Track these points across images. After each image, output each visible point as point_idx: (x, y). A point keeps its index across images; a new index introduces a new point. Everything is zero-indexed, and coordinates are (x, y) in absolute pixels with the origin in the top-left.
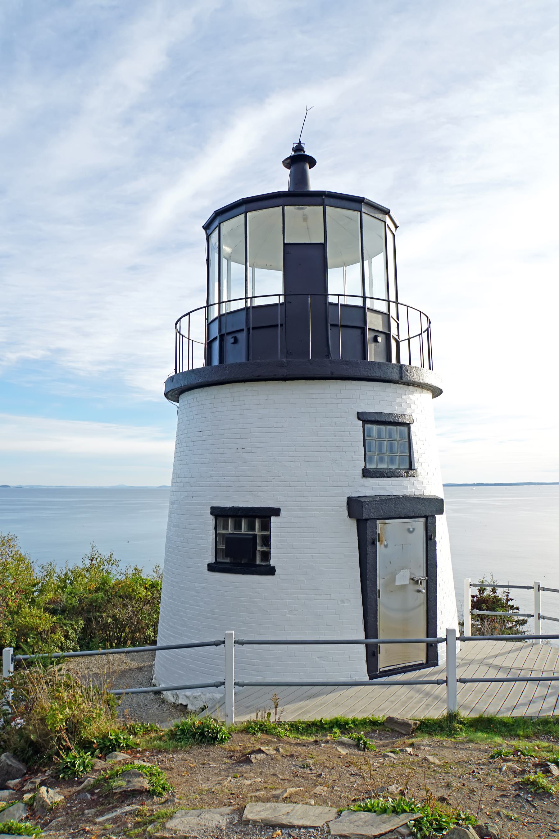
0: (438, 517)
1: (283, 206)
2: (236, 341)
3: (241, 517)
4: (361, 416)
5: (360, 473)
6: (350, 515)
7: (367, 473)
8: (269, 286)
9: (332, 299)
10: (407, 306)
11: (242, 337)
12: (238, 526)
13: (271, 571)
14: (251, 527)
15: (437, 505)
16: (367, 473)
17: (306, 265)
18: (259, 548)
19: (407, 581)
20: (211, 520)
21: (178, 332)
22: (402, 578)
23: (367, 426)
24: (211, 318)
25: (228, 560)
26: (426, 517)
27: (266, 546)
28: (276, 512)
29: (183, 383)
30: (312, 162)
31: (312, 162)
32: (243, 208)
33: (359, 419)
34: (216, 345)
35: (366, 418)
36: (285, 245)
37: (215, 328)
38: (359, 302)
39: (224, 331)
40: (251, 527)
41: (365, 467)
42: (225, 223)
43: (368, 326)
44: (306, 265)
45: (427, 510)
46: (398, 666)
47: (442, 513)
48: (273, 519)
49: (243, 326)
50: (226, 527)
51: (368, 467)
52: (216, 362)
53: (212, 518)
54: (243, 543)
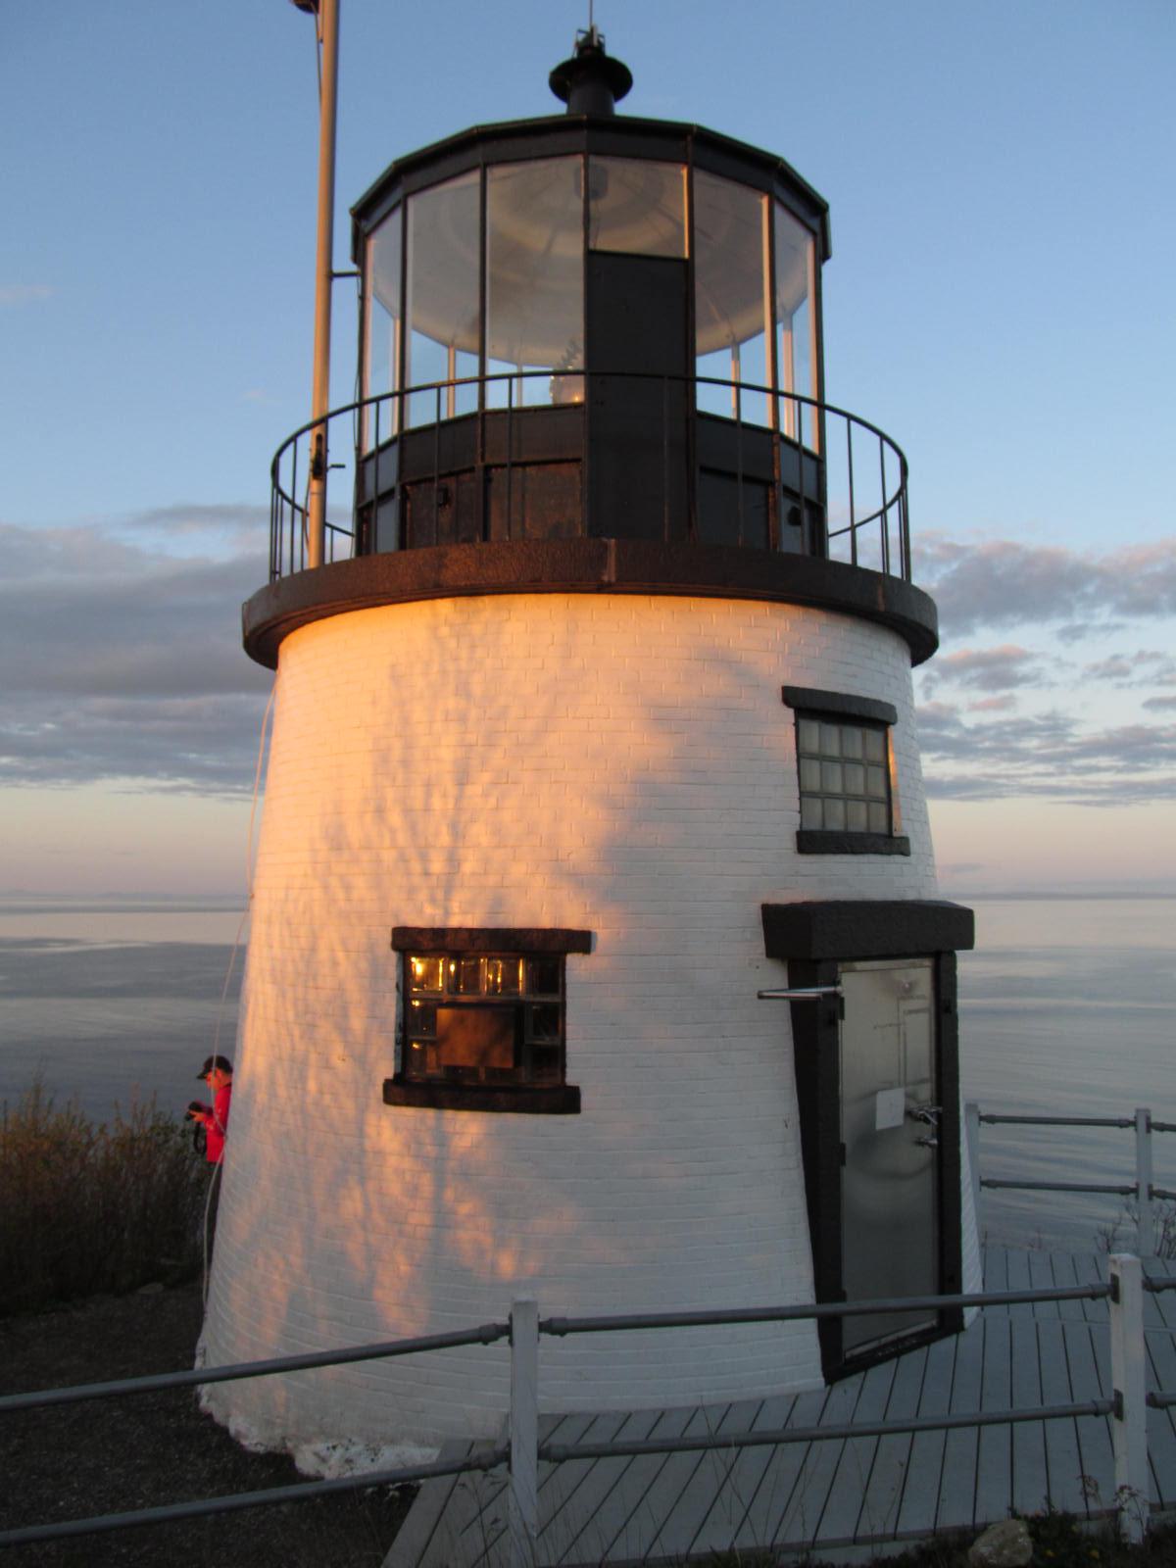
0: (959, 953)
2: (446, 499)
5: (790, 843)
6: (773, 951)
7: (809, 842)
9: (711, 401)
13: (568, 1101)
16: (809, 842)
19: (898, 1119)
22: (889, 1110)
24: (384, 438)
32: (477, 154)
36: (591, 255)
37: (390, 460)
41: (801, 825)
44: (643, 317)
46: (884, 1341)
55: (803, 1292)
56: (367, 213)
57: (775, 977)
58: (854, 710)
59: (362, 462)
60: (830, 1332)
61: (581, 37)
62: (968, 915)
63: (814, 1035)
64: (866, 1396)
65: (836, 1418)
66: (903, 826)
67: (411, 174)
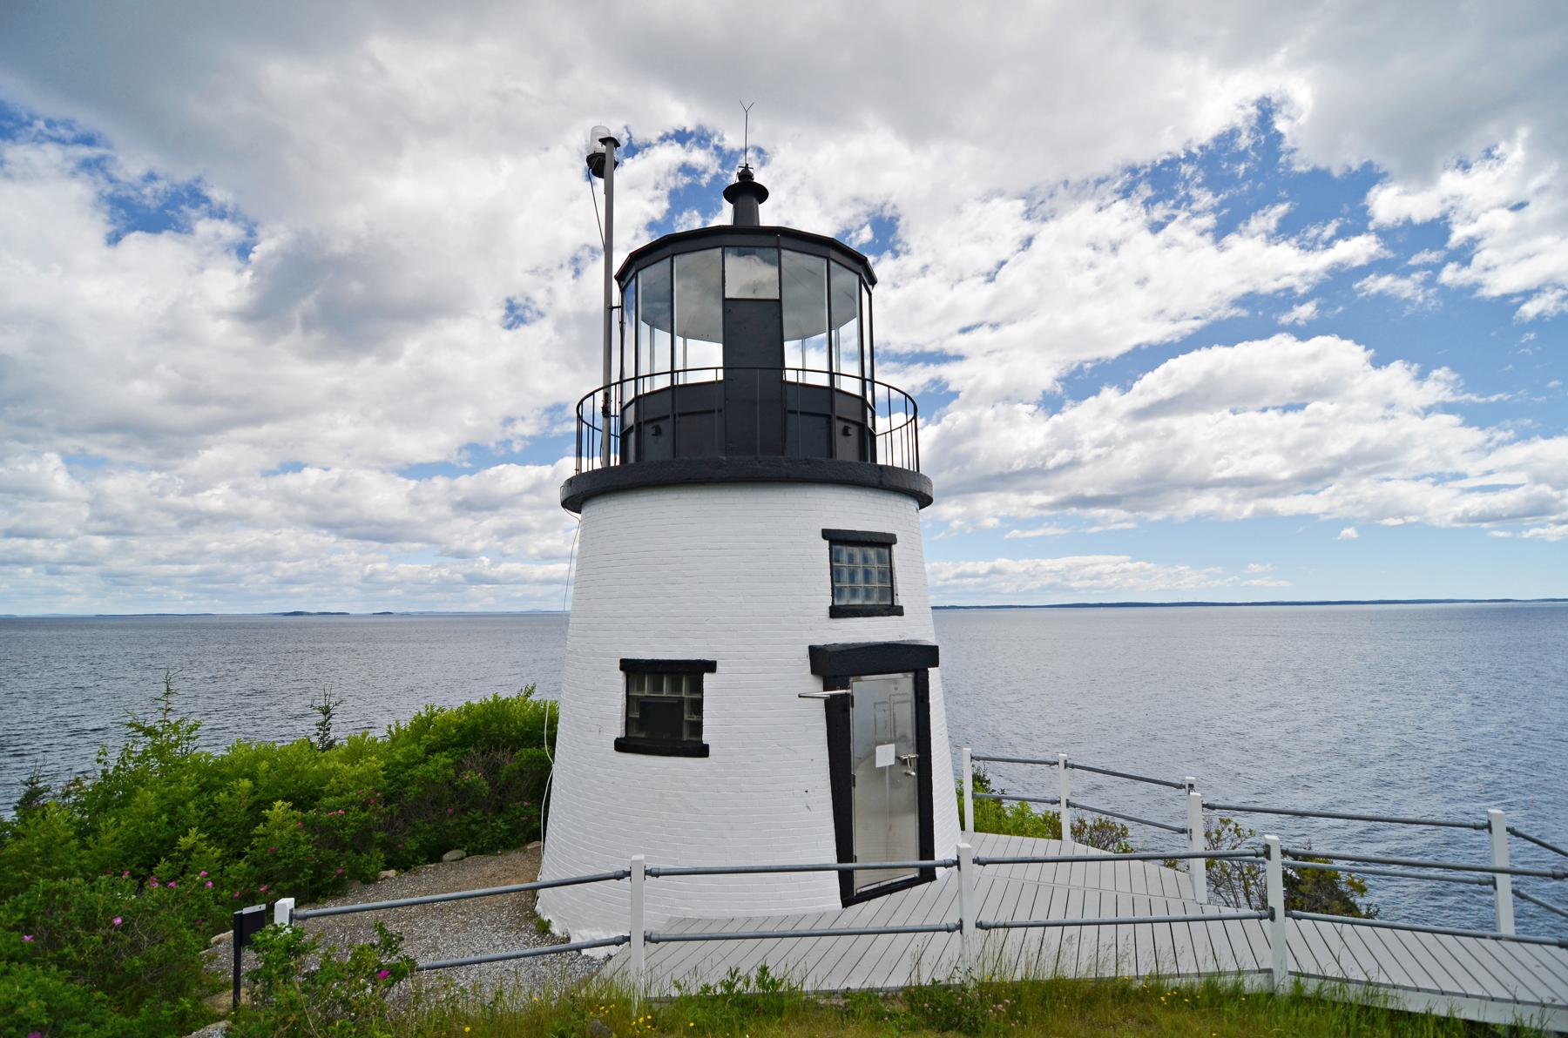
1: (724, 247)
2: (658, 432)
3: (662, 673)
4: (826, 534)
6: (813, 672)
7: (836, 612)
8: (704, 360)
9: (790, 376)
11: (666, 426)
13: (702, 751)
14: (676, 687)
15: (930, 655)
16: (836, 612)
17: (753, 331)
18: (686, 717)
20: (620, 677)
22: (885, 756)
24: (627, 400)
25: (643, 735)
28: (711, 666)
30: (761, 194)
31: (761, 194)
32: (669, 250)
34: (632, 436)
35: (835, 538)
36: (725, 300)
38: (823, 380)
40: (676, 687)
42: (645, 271)
43: (838, 412)
44: (753, 331)
45: (916, 660)
48: (706, 676)
50: (641, 688)
52: (632, 459)
53: (621, 673)
54: (664, 709)
55: (831, 857)
56: (621, 277)
57: (814, 686)
58: (862, 538)
59: (623, 410)
60: (846, 879)
62: (936, 649)
63: (838, 715)
64: (864, 913)
65: (842, 925)
67: (638, 259)
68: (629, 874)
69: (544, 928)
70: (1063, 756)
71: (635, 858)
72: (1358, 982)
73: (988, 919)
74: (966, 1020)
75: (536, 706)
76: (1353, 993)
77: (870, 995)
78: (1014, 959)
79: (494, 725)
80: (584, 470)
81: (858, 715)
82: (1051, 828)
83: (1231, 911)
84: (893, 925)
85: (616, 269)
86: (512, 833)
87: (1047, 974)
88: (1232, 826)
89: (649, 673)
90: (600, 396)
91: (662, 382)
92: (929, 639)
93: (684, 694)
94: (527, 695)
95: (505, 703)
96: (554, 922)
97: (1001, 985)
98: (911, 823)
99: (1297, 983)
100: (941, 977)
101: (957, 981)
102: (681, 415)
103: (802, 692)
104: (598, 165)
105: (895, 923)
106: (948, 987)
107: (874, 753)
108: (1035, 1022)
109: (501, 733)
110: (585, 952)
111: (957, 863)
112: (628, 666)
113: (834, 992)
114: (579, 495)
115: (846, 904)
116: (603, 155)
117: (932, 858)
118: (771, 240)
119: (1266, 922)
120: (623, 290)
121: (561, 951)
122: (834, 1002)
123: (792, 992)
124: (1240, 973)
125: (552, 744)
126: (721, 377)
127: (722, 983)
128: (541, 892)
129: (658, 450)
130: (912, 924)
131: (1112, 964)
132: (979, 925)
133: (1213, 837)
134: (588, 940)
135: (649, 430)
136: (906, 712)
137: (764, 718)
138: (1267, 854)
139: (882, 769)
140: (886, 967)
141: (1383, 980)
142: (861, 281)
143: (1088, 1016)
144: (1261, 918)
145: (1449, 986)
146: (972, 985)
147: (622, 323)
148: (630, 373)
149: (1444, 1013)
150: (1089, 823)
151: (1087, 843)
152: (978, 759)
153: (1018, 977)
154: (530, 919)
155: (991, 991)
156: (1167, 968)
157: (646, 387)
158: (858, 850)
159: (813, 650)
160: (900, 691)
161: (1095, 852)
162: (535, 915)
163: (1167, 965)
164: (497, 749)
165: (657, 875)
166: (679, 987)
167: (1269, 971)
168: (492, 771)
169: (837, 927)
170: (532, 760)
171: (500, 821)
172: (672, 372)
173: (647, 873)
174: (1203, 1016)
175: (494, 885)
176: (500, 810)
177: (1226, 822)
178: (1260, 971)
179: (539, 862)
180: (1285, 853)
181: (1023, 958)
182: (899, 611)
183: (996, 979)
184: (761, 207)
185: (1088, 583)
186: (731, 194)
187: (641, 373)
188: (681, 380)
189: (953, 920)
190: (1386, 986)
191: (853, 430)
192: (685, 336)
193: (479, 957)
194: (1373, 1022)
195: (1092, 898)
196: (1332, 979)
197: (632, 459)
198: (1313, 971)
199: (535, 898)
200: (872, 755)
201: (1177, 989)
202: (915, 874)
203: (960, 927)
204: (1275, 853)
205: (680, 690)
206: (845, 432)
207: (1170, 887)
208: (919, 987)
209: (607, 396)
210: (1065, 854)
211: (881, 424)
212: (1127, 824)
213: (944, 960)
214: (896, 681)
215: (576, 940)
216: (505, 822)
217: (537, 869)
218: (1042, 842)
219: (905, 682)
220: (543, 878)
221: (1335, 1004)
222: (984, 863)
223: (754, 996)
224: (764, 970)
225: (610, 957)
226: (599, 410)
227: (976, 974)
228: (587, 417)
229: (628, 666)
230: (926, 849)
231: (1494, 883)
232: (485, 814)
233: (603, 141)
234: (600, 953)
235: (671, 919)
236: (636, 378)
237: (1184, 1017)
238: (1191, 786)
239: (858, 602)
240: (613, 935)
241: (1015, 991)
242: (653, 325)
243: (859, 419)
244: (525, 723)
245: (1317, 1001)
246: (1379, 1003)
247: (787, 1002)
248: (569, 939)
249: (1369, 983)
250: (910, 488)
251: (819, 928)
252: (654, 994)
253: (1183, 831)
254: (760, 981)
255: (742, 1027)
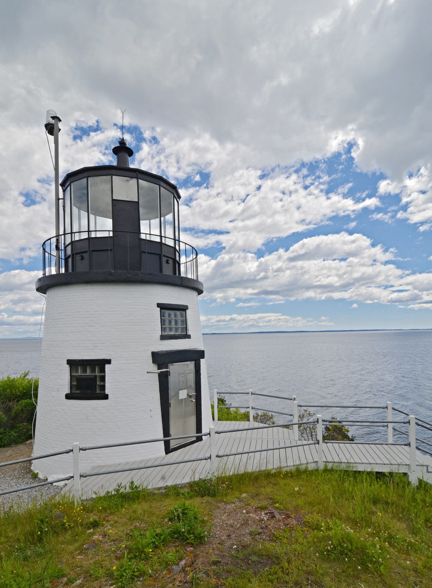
4: (159, 305)
5: (159, 337)
6: (154, 362)
7: (163, 338)
8: (104, 226)
10: (186, 244)
12: (85, 371)
13: (106, 397)
14: (93, 371)
15: (201, 354)
16: (163, 338)
18: (98, 383)
20: (67, 367)
21: (44, 249)
23: (162, 311)
26: (195, 360)
27: (102, 381)
28: (109, 362)
29: (47, 282)
30: (130, 153)
31: (130, 153)
33: (158, 307)
34: (70, 260)
35: (162, 307)
38: (158, 239)
39: (74, 252)
40: (93, 371)
45: (196, 356)
47: (203, 357)
48: (107, 366)
49: (87, 249)
50: (77, 371)
51: (163, 334)
52: (70, 270)
57: (154, 368)
58: (174, 307)
59: (65, 247)
61: (120, 140)
62: (204, 351)
63: (164, 379)
66: (190, 332)
68: (72, 450)
69: (35, 476)
70: (251, 390)
71: (75, 444)
72: (345, 463)
73: (221, 454)
74: (211, 492)
75: (29, 382)
76: (343, 467)
77: (175, 487)
78: (230, 467)
79: (8, 390)
80: (47, 274)
81: (171, 379)
82: (246, 417)
83: (305, 442)
84: (185, 459)
85: (60, 181)
86: (19, 437)
87: (242, 471)
88: (308, 412)
89: (80, 365)
90: (54, 240)
91: (85, 236)
92: (201, 348)
93: (97, 374)
94: (25, 376)
95: (13, 380)
96: (40, 473)
97: (224, 477)
98: (193, 420)
99: (326, 465)
100: (202, 477)
101: (209, 478)
102: (93, 251)
103: (148, 371)
104: (51, 129)
105: (186, 459)
106: (206, 480)
107: (178, 393)
108: (236, 489)
109: (12, 394)
110: (54, 484)
111: (209, 434)
112: (70, 362)
113: (161, 488)
114: (45, 285)
115: (167, 453)
116: (53, 125)
117: (201, 433)
118: (134, 174)
119: (317, 445)
120: (64, 191)
121: (43, 485)
122: (161, 491)
123: (144, 490)
124: (307, 463)
125: (36, 396)
126: (111, 234)
127: (114, 490)
128: (33, 461)
129: (82, 266)
130: (193, 458)
131: (264, 465)
132: (217, 456)
133: (301, 417)
134: (56, 479)
135: (78, 257)
136: (192, 377)
137: (132, 383)
138: (318, 422)
139: (182, 400)
140: (182, 476)
141: (352, 461)
142: (174, 197)
143: (256, 484)
144: (315, 444)
145: (372, 461)
146: (214, 479)
147: (64, 206)
148: (68, 230)
149: (369, 470)
150: (260, 414)
151: (259, 422)
152: (220, 393)
153: (231, 474)
154: (29, 473)
155: (221, 480)
156: (283, 464)
157: (77, 237)
158: (172, 432)
159: (154, 354)
160: (189, 369)
161: (261, 425)
162: (31, 471)
163: (283, 463)
164: (10, 401)
165: (85, 450)
166: (96, 493)
167: (317, 462)
168: (8, 410)
169: (163, 463)
170: (27, 405)
171: (13, 433)
172: (89, 231)
173: (80, 449)
174: (294, 480)
175: (11, 460)
176: (13, 427)
177: (306, 411)
178: (314, 462)
179: (32, 449)
180: (323, 421)
181: (233, 466)
182: (189, 337)
183: (223, 475)
184: (130, 159)
185: (265, 324)
186: (116, 151)
187: (74, 231)
188: (93, 235)
189: (208, 455)
190: (353, 463)
191: (171, 261)
192: (96, 215)
193: (4, 492)
194: (348, 476)
195: (259, 442)
196: (336, 462)
197: (70, 270)
198: (331, 461)
199: (31, 464)
200: (178, 394)
201: (286, 471)
202: (195, 439)
203: (210, 458)
204: (320, 421)
205: (95, 372)
206: (167, 262)
207: (286, 436)
208: (194, 482)
209: (58, 240)
210: (251, 427)
211: (183, 259)
212: (273, 414)
213: (204, 471)
214: (187, 365)
215: (50, 480)
216: (16, 432)
217: (31, 452)
218: (242, 423)
219: (191, 365)
220: (34, 455)
221: (337, 471)
222: (219, 433)
223: (128, 493)
224: (132, 483)
225: (66, 485)
226: (54, 246)
227: (216, 474)
228: (48, 249)
229: (70, 362)
230: (199, 429)
231: (387, 426)
232: (5, 429)
233: (53, 118)
234: (62, 484)
235: (93, 467)
236: (71, 233)
237: (288, 481)
238: (294, 399)
239: (172, 333)
240: (68, 476)
241: (230, 479)
242: (79, 209)
243: (173, 257)
244: (24, 389)
245: (331, 471)
246: (350, 469)
247: (141, 494)
248: (47, 479)
249: (348, 463)
250: (194, 286)
251: (155, 464)
252: (84, 498)
253: (291, 415)
254: (131, 487)
255: (122, 506)
